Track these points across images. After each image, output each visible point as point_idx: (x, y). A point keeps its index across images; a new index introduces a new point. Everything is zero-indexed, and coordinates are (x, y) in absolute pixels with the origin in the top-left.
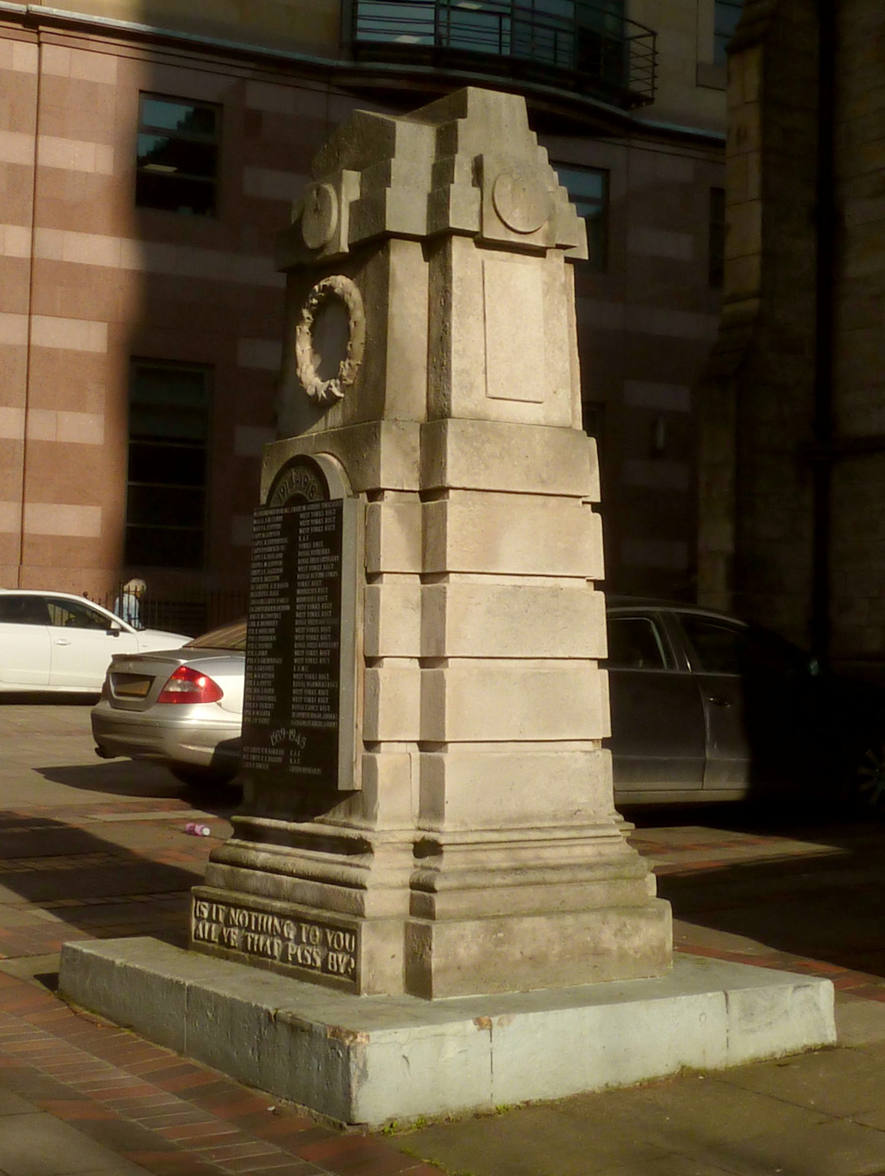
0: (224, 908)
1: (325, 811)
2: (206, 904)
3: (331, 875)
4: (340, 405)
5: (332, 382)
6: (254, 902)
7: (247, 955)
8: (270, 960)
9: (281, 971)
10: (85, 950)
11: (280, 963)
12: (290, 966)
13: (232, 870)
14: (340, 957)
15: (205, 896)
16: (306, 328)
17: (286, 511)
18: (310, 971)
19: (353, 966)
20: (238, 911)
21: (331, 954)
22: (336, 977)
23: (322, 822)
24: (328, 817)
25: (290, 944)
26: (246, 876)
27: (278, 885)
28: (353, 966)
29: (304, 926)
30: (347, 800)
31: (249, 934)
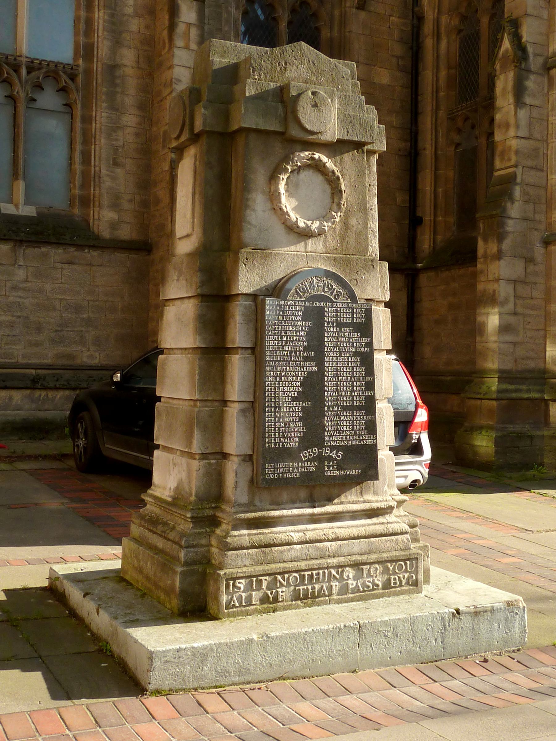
0: (267, 578)
1: (339, 496)
2: (242, 581)
3: (379, 533)
4: (322, 238)
5: (325, 224)
6: (306, 565)
7: (299, 602)
8: (327, 598)
9: (339, 602)
10: (195, 645)
11: (339, 597)
12: (352, 595)
13: (263, 552)
14: (401, 576)
15: (242, 575)
16: (285, 177)
17: (307, 304)
18: (372, 592)
19: (414, 578)
20: (286, 576)
21: (392, 577)
22: (399, 589)
23: (342, 503)
24: (343, 498)
25: (350, 582)
26: (281, 552)
27: (327, 549)
28: (414, 578)
29: (364, 567)
30: (358, 487)
31: (301, 588)
